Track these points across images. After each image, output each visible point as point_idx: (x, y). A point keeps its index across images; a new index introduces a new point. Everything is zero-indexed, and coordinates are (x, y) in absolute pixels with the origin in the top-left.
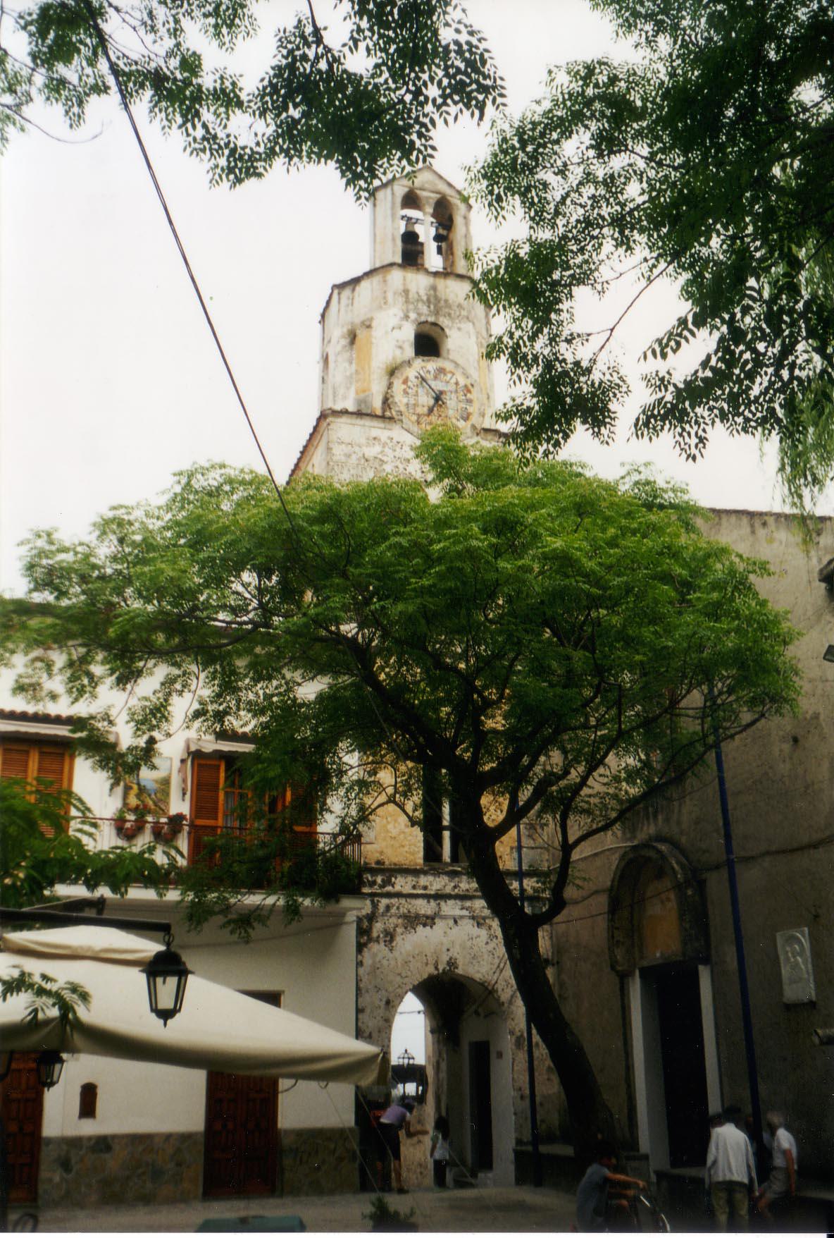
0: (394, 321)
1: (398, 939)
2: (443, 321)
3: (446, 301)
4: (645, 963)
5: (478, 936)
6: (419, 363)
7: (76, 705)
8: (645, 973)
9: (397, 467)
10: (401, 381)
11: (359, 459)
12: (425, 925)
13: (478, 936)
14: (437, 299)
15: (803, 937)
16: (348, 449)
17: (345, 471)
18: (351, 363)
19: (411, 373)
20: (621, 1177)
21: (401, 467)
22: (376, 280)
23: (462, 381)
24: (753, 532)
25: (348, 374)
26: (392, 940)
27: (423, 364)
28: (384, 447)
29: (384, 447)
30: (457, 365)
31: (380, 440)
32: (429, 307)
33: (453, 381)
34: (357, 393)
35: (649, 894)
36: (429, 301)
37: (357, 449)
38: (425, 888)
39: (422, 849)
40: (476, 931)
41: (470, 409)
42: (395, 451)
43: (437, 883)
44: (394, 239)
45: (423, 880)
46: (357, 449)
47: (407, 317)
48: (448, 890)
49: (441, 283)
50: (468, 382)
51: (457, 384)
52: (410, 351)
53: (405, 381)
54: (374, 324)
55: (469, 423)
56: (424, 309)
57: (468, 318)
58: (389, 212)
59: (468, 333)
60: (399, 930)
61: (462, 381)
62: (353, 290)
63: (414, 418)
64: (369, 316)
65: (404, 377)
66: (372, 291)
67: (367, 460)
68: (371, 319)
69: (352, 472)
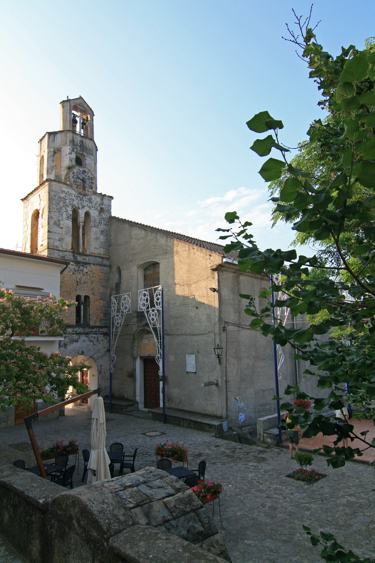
0: (68, 151)
1: (68, 346)
2: (85, 154)
3: (86, 147)
4: (142, 355)
5: (90, 344)
6: (77, 168)
7: (321, 472)
8: (141, 358)
9: (70, 202)
10: (72, 173)
11: (58, 198)
12: (75, 342)
13: (90, 344)
14: (83, 146)
15: (193, 357)
16: (55, 194)
17: (54, 201)
18: (53, 162)
19: (75, 170)
20: (244, 466)
21: (71, 201)
22: (63, 134)
23: (91, 176)
24: (189, 250)
25: (52, 165)
26: (66, 346)
27: (79, 168)
28: (66, 194)
29: (66, 194)
30: (89, 170)
31: (65, 192)
32: (80, 148)
33: (88, 175)
34: (55, 173)
35: (144, 337)
36: (80, 146)
37: (58, 194)
38: (76, 331)
39: (75, 320)
40: (89, 343)
41: (93, 186)
42: (69, 196)
43: (80, 330)
44: (70, 122)
45: (75, 329)
46: (58, 194)
47: (73, 150)
48: (82, 331)
49: (84, 140)
50: (93, 176)
51: (89, 176)
52: (74, 163)
53: (74, 173)
54: (62, 150)
55: (92, 190)
56: (79, 149)
57: (92, 154)
58: (68, 111)
59: (92, 159)
60: (68, 343)
61: (91, 176)
62: (54, 136)
63: (76, 186)
64: (60, 146)
65: (73, 172)
66: (62, 138)
67: (61, 198)
68: (61, 148)
69: (56, 201)
